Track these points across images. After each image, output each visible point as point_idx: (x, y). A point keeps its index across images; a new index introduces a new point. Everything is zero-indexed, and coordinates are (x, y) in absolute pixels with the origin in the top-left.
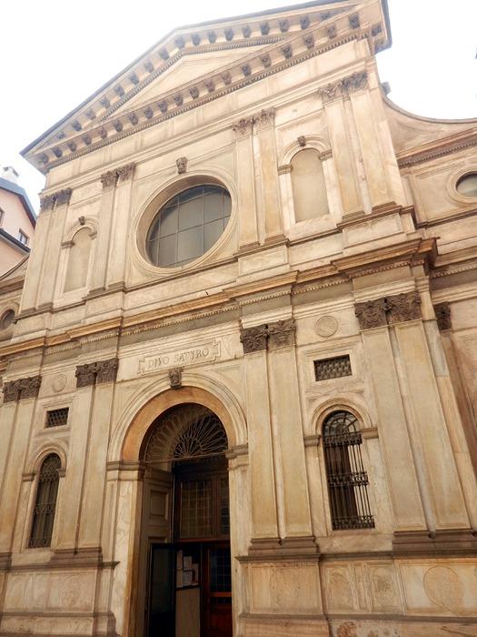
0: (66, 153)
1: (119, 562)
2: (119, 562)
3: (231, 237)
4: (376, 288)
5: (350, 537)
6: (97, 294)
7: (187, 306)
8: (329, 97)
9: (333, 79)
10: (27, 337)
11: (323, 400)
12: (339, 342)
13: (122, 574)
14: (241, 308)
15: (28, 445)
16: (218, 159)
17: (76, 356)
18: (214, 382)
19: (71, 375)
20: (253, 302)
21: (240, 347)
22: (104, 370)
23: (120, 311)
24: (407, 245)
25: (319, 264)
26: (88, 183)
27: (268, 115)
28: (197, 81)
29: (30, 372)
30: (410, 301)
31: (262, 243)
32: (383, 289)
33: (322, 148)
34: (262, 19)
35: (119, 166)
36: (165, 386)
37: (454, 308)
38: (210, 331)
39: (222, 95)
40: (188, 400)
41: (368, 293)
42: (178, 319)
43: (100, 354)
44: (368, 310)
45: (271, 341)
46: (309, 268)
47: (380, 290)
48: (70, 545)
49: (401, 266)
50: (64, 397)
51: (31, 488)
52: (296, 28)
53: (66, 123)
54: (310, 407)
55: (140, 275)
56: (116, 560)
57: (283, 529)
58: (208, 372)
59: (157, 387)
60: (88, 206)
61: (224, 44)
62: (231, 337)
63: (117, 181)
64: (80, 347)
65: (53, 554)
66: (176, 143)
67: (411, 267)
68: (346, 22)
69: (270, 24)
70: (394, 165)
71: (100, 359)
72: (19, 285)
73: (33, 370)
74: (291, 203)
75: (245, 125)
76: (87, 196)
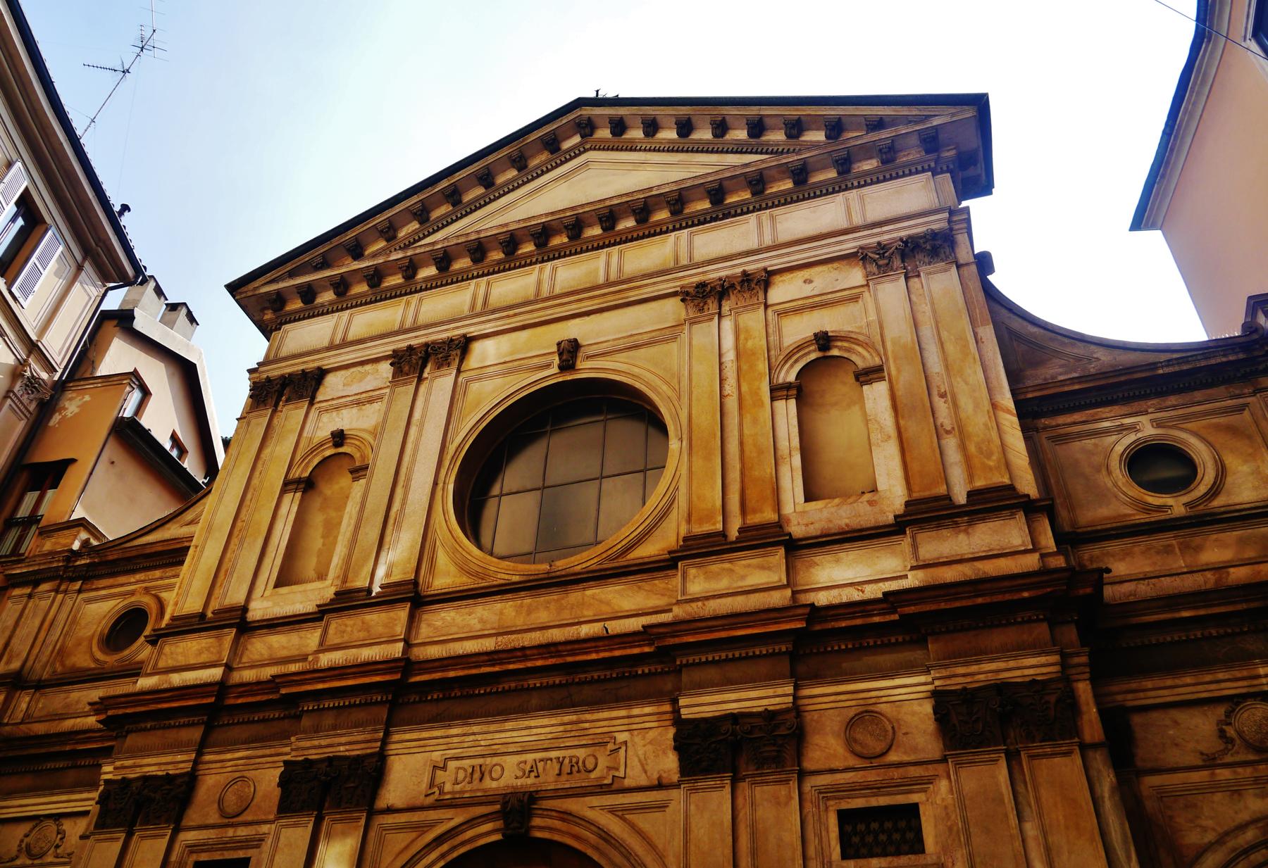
3: (664, 514)
4: (978, 662)
8: (879, 267)
9: (889, 235)
10: (177, 679)
12: (896, 774)
14: (678, 671)
16: (642, 351)
17: (284, 736)
18: (605, 836)
19: (268, 779)
20: (707, 662)
21: (670, 763)
24: (1045, 578)
25: (855, 595)
26: (362, 363)
28: (616, 202)
29: (175, 762)
30: (1053, 699)
31: (733, 533)
32: (993, 666)
33: (863, 358)
34: (754, 111)
38: (606, 714)
39: (661, 233)
41: (961, 670)
43: (343, 740)
46: (836, 601)
49: (1030, 621)
50: (242, 832)
52: (818, 136)
53: (336, 241)
55: (453, 569)
58: (591, 808)
59: (470, 834)
60: (355, 410)
61: (671, 141)
62: (651, 734)
64: (298, 717)
68: (914, 140)
69: (767, 121)
70: (1008, 412)
72: (174, 555)
73: (179, 758)
74: (797, 460)
76: (355, 388)
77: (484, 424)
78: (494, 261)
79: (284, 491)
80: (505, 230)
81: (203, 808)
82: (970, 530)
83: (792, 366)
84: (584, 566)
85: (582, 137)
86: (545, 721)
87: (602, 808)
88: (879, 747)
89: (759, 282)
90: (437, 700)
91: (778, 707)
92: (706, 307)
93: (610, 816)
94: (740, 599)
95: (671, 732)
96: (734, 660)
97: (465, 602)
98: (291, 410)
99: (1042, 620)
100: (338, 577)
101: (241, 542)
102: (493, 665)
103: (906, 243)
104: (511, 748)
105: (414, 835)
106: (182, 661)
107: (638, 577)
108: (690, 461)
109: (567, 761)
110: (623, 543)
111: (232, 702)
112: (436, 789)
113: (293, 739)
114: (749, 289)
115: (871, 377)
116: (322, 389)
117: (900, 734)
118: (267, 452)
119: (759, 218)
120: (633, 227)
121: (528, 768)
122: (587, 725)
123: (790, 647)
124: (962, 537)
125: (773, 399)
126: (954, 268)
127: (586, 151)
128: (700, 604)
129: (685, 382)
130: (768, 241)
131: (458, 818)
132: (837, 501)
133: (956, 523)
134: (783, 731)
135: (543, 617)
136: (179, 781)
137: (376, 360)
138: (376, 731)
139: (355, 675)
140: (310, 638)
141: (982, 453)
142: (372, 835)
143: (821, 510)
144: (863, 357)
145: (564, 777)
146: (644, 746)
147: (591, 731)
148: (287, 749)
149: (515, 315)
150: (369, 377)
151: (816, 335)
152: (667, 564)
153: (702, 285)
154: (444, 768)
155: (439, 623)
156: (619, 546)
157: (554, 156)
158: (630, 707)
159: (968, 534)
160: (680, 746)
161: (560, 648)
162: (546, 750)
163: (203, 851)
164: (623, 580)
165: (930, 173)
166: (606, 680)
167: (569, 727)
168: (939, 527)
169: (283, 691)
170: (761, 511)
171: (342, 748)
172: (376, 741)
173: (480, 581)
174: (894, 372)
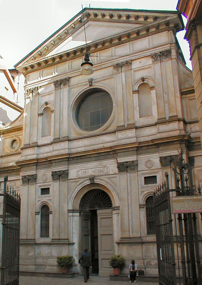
1: (75, 243)
2: (75, 243)
5: (152, 237)
6: (56, 141)
8: (155, 59)
9: (157, 50)
11: (146, 192)
12: (153, 171)
13: (76, 246)
14: (117, 153)
15: (35, 201)
17: (50, 167)
21: (116, 170)
22: (63, 174)
23: (68, 149)
27: (128, 63)
29: (33, 172)
30: (179, 158)
35: (62, 78)
36: (88, 182)
37: (195, 158)
40: (97, 188)
41: (165, 153)
44: (164, 160)
47: (169, 152)
48: (57, 237)
51: (39, 217)
52: (142, 19)
54: (142, 194)
56: (74, 242)
57: (131, 234)
59: (85, 183)
65: (51, 240)
67: (180, 145)
70: (178, 98)
73: (33, 171)
75: (118, 66)
82: (169, 125)
83: (137, 85)
85: (87, 18)
86: (95, 163)
89: (129, 63)
92: (119, 70)
95: (117, 164)
99: (179, 143)
103: (160, 53)
105: (76, 183)
109: (100, 170)
113: (52, 168)
114: (128, 65)
122: (102, 163)
123: (136, 149)
125: (133, 94)
126: (170, 60)
127: (89, 21)
130: (132, 52)
131: (83, 180)
132: (145, 118)
133: (166, 124)
138: (66, 166)
145: (99, 173)
146: (112, 167)
147: (103, 165)
148: (51, 169)
152: (114, 132)
153: (117, 64)
155: (74, 144)
159: (168, 126)
160: (118, 167)
163: (41, 187)
165: (167, 31)
169: (49, 160)
174: (157, 88)
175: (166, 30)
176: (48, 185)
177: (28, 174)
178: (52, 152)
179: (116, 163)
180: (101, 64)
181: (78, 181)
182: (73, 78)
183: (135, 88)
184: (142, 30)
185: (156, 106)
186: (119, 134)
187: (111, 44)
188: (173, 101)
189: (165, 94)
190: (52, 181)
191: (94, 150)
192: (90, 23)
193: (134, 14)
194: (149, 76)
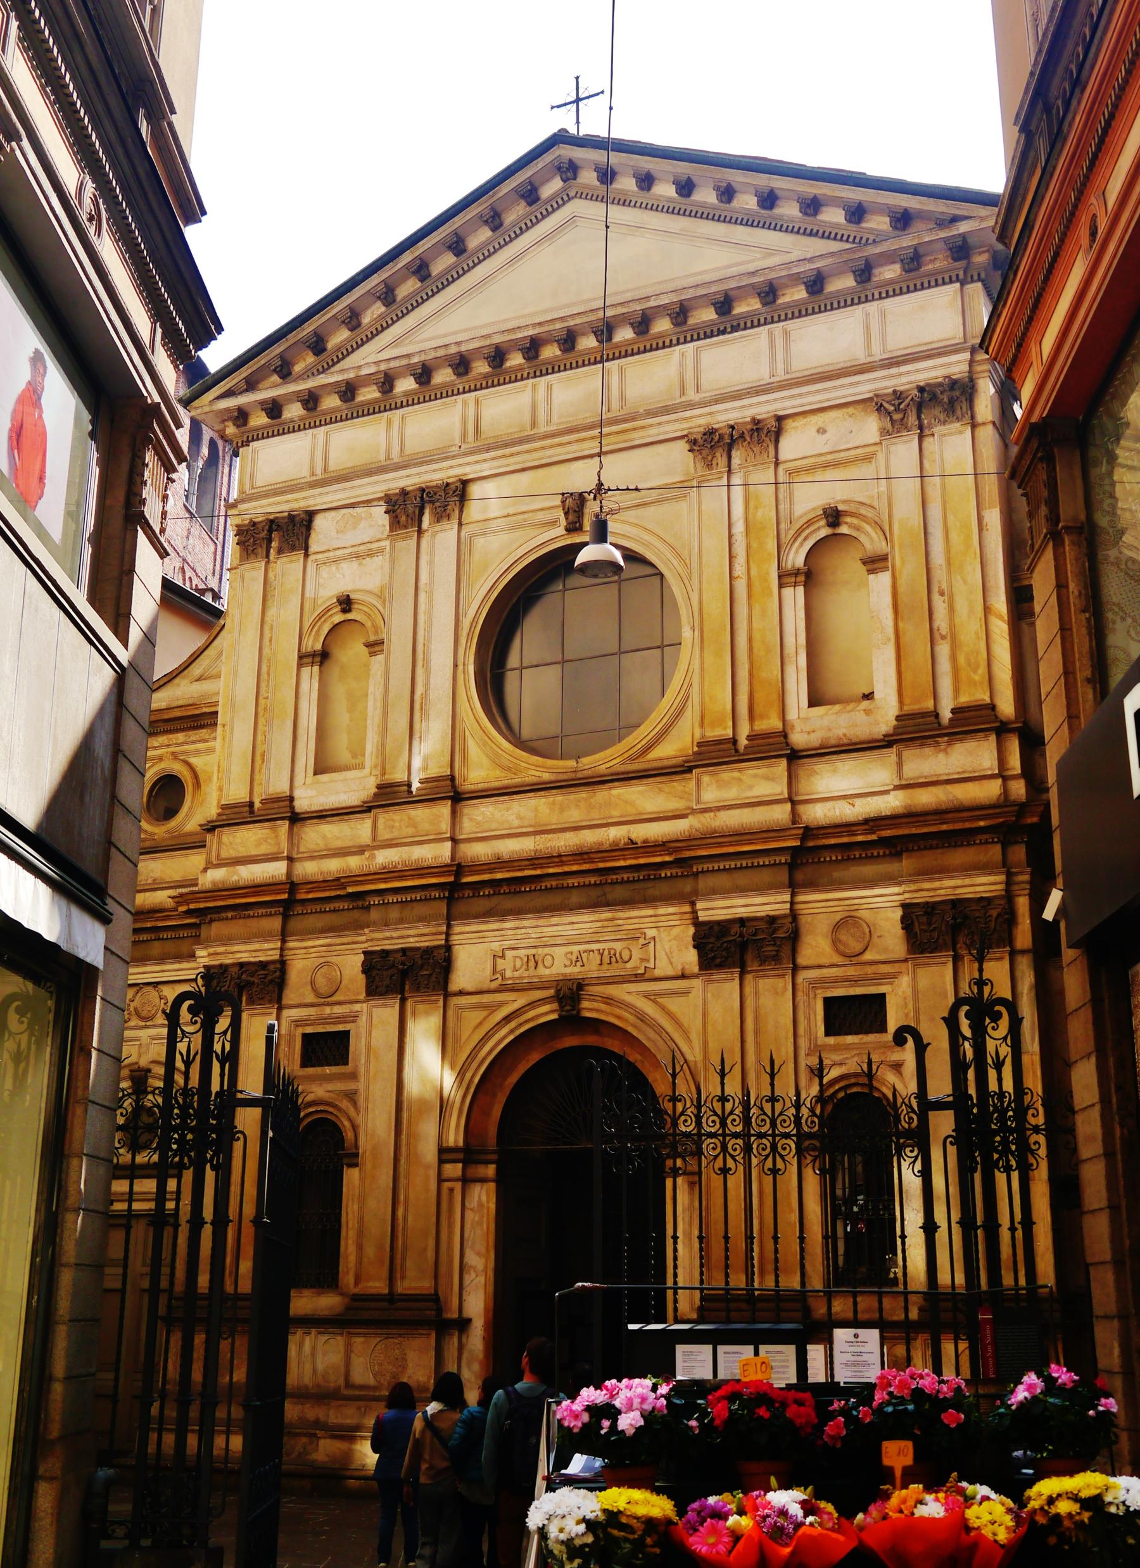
0: (293, 411)
3: (679, 713)
4: (940, 879)
7: (591, 861)
12: (870, 970)
16: (651, 509)
17: (358, 926)
18: (642, 1017)
19: (352, 964)
21: (691, 957)
22: (422, 967)
26: (352, 506)
30: (994, 913)
33: (872, 542)
40: (591, 1040)
41: (926, 885)
42: (570, 881)
45: (749, 957)
49: (987, 842)
50: (338, 1010)
52: (834, 216)
53: (292, 338)
55: (485, 761)
59: (531, 1014)
60: (355, 564)
62: (675, 931)
63: (421, 514)
64: (368, 908)
66: (558, 450)
70: (1000, 617)
71: (412, 942)
73: (266, 946)
77: (495, 594)
78: (479, 374)
79: (300, 665)
80: (488, 342)
81: (297, 988)
82: (949, 750)
83: (801, 544)
84: (608, 765)
86: (585, 918)
87: (638, 993)
88: (856, 946)
90: (489, 895)
91: (777, 913)
92: (714, 463)
93: (644, 999)
94: (746, 811)
96: (741, 868)
97: (501, 798)
98: (286, 563)
99: (993, 842)
100: (376, 766)
101: (269, 723)
102: (535, 869)
104: (559, 941)
105: (485, 1013)
106: (242, 851)
107: (658, 779)
108: (702, 657)
109: (606, 952)
110: (643, 742)
111: (303, 896)
112: (498, 976)
113: (366, 931)
115: (876, 566)
116: (313, 535)
117: (875, 939)
118: (271, 613)
119: (771, 334)
120: (633, 339)
121: (574, 959)
123: (789, 858)
124: (941, 756)
125: (781, 586)
127: (569, 199)
128: (712, 814)
129: (695, 558)
130: (781, 376)
131: (521, 1000)
132: (837, 707)
133: (937, 742)
134: (781, 934)
135: (575, 815)
136: (272, 967)
137: (367, 503)
138: (439, 925)
139: (413, 877)
140: (361, 829)
141: (969, 665)
142: (450, 1013)
143: (822, 717)
144: (871, 539)
145: (605, 967)
148: (363, 938)
149: (512, 455)
150: (363, 524)
151: (825, 511)
153: (710, 432)
154: (503, 957)
155: (480, 818)
156: (639, 746)
157: (534, 207)
158: (656, 907)
159: (947, 753)
160: (699, 943)
161: (592, 856)
162: (588, 942)
164: (645, 781)
165: (958, 285)
166: (634, 881)
167: (606, 923)
168: (922, 745)
169: (350, 890)
170: (769, 718)
171: (412, 940)
172: (441, 934)
173: (513, 776)
175: (954, 278)
176: (342, 1019)
177: (239, 955)
178: (367, 854)
179: (689, 922)
180: (627, 426)
181: (500, 1005)
182: (479, 482)
183: (791, 556)
184: (840, 272)
185: (890, 653)
186: (706, 779)
187: (678, 329)
188: (976, 633)
189: (937, 600)
190: (363, 996)
191: (581, 855)
192: (576, 206)
193: (800, 188)
194: (863, 504)
